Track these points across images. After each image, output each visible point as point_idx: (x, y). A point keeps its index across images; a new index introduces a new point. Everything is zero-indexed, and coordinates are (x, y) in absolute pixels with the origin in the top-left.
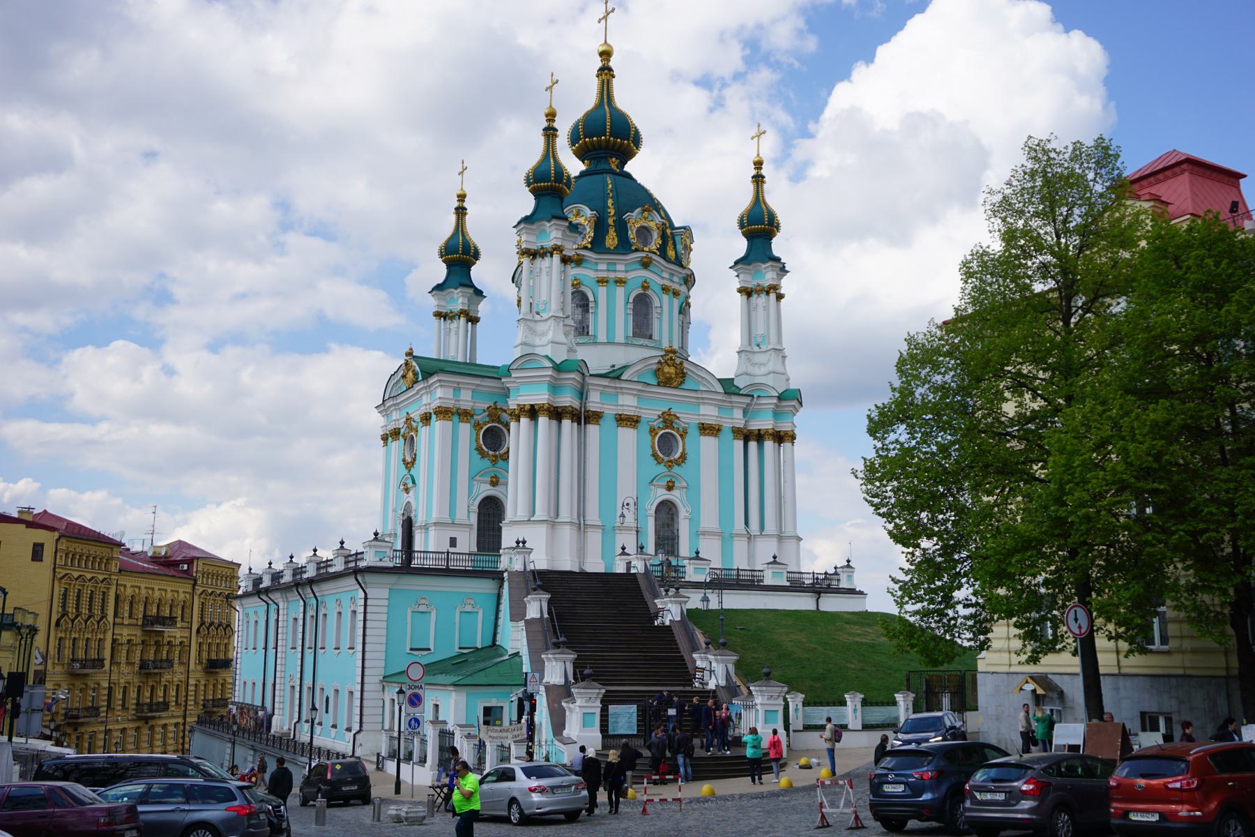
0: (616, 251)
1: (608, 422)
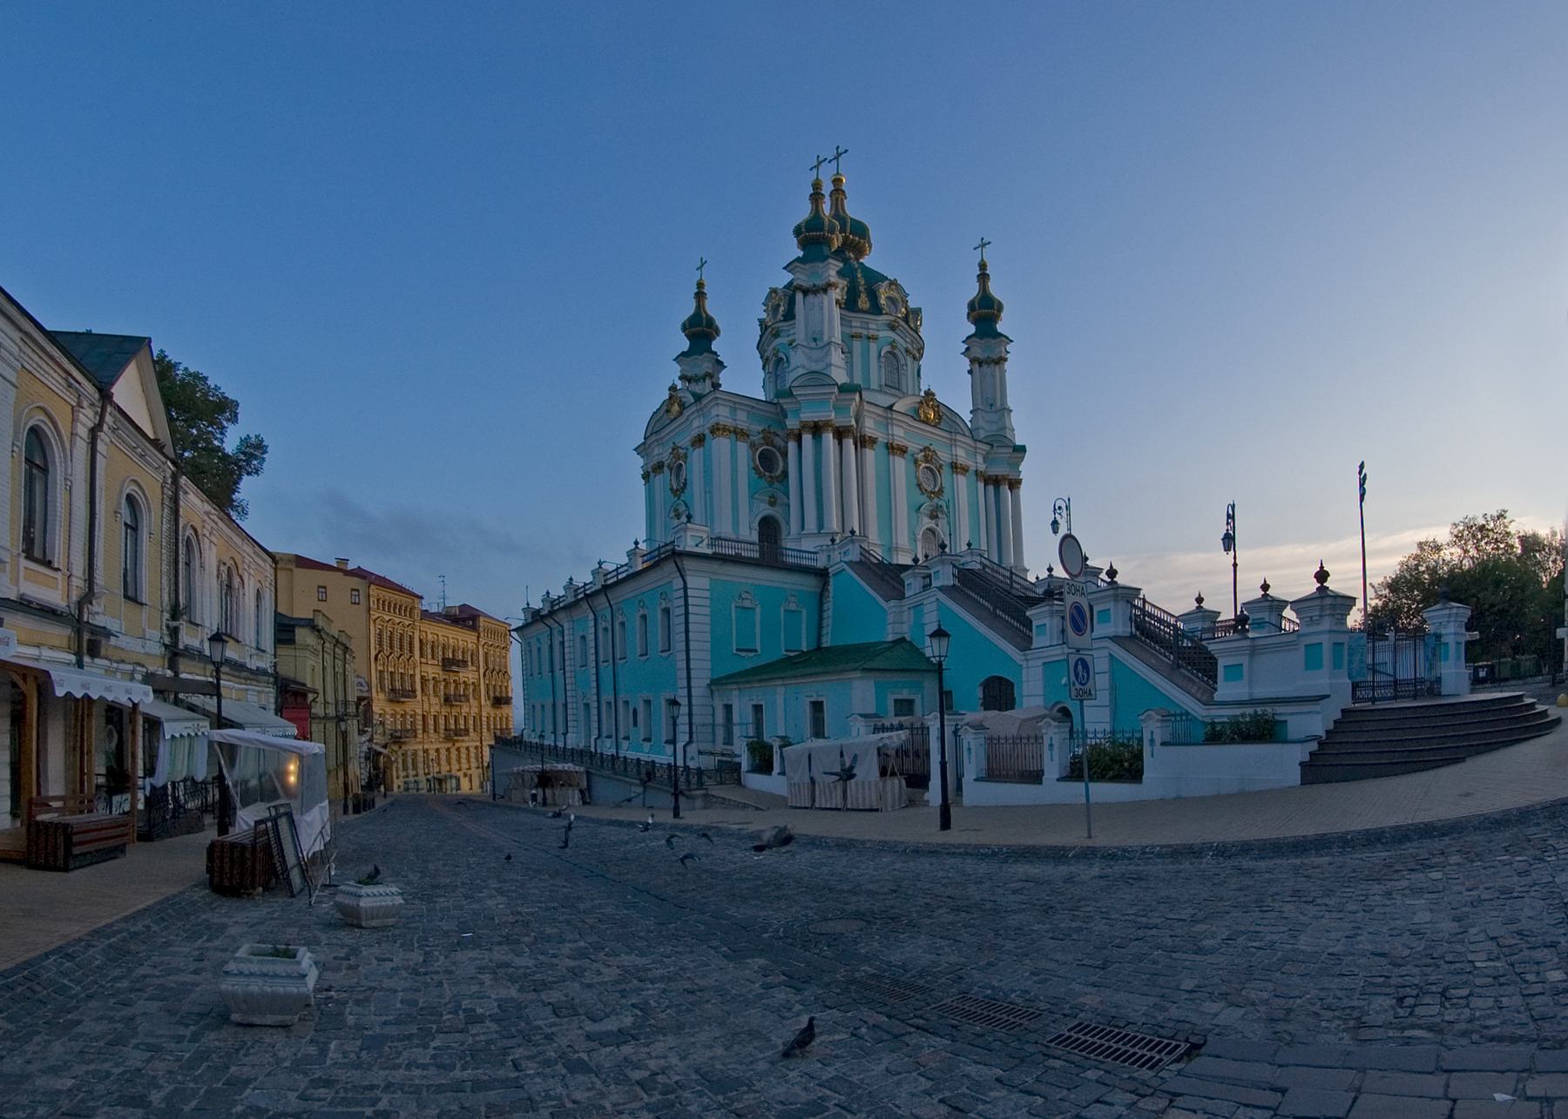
1: (879, 447)
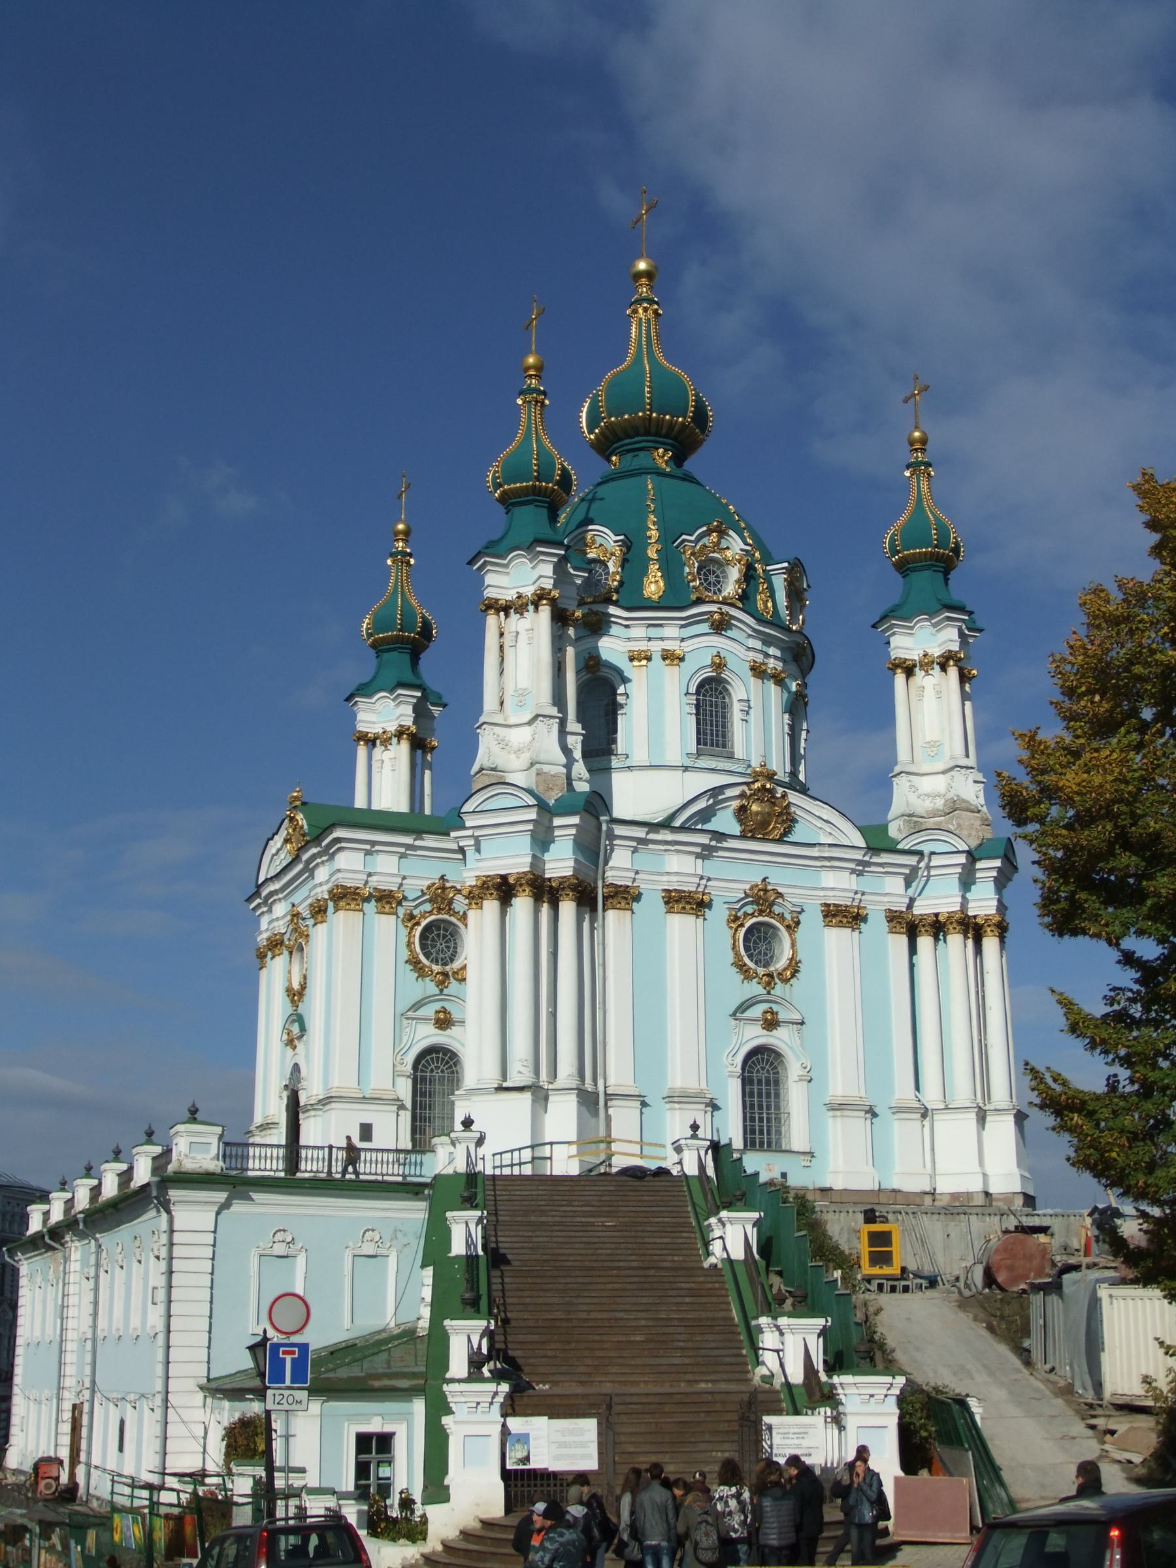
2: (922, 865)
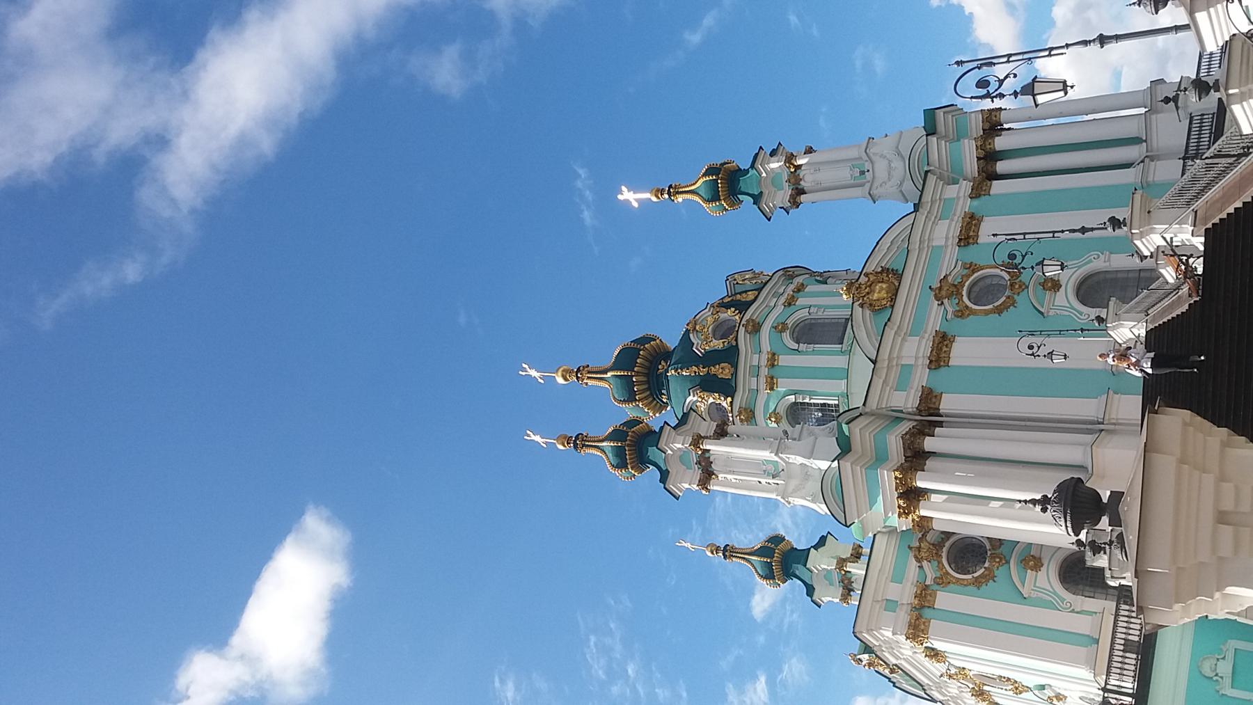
0: (735, 366)
2: (938, 171)
